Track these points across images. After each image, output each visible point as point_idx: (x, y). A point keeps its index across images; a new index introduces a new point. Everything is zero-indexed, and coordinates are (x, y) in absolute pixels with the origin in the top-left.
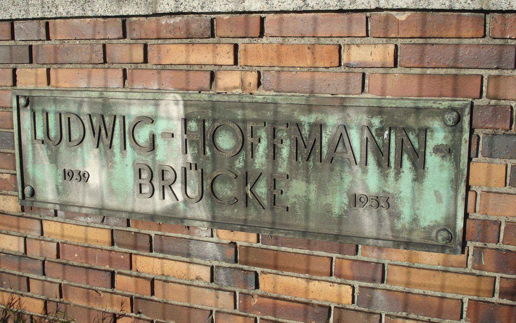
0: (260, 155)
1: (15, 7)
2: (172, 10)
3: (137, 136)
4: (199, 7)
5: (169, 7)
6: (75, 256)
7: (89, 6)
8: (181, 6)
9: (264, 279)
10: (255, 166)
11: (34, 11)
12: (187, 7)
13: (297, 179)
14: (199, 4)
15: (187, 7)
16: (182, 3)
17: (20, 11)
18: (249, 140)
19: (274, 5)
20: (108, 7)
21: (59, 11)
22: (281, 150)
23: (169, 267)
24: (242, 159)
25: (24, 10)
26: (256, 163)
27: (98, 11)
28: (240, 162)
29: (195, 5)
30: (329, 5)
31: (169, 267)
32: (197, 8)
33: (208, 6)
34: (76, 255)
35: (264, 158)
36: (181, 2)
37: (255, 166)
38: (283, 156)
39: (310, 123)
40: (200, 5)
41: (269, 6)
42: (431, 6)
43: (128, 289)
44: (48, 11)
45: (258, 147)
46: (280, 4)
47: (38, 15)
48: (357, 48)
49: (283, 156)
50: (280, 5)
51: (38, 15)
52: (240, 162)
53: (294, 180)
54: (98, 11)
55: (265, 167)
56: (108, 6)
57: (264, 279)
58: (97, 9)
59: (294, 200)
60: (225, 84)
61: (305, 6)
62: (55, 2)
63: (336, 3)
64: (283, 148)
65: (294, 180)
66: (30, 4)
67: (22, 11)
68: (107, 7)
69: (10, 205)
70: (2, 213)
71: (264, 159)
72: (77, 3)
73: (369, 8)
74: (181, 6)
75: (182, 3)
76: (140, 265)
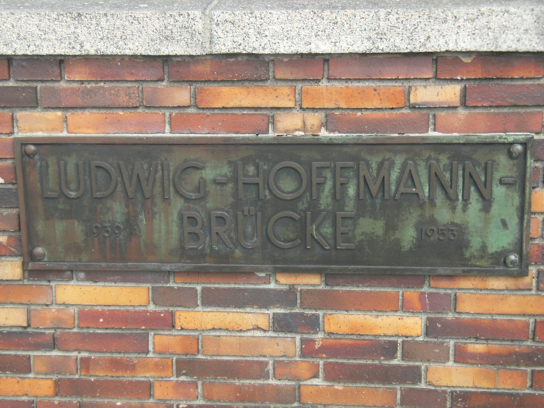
0: (325, 195)
1: (22, 41)
2: (229, 51)
3: (184, 183)
4: (261, 48)
5: (225, 48)
6: (99, 321)
7: (125, 44)
8: (240, 47)
9: (328, 320)
10: (319, 207)
11: (49, 46)
12: (247, 48)
13: (364, 217)
14: (260, 45)
15: (247, 48)
16: (241, 44)
17: (29, 46)
18: (315, 180)
19: (343, 48)
20: (151, 46)
21: (85, 48)
22: (347, 189)
23: (221, 319)
24: (305, 200)
25: (35, 45)
26: (321, 204)
27: (137, 50)
28: (303, 203)
29: (256, 46)
30: (399, 48)
31: (221, 319)
32: (258, 49)
33: (270, 48)
34: (101, 320)
35: (330, 198)
36: (239, 43)
37: (319, 207)
38: (349, 195)
39: (481, 209)
40: (261, 46)
41: (337, 48)
42: (498, 49)
43: (169, 349)
44: (69, 48)
45: (323, 188)
46: (349, 46)
47: (55, 51)
48: (424, 89)
49: (349, 195)
50: (349, 48)
51: (55, 51)
52: (303, 203)
53: (361, 218)
54: (137, 50)
55: (331, 207)
56: (151, 45)
57: (328, 320)
58: (137, 48)
59: (361, 237)
60: (285, 127)
61: (375, 48)
62: (79, 38)
63: (406, 46)
64: (349, 187)
65: (361, 218)
66: (44, 39)
67: (31, 47)
68: (149, 46)
69: (7, 272)
70: (2, 280)
71: (329, 200)
72: (110, 40)
73: (439, 51)
74: (240, 47)
75: (241, 44)
76: (185, 321)
